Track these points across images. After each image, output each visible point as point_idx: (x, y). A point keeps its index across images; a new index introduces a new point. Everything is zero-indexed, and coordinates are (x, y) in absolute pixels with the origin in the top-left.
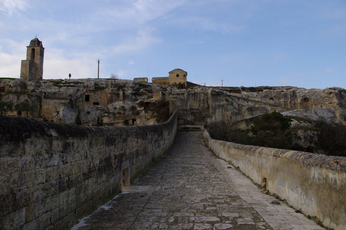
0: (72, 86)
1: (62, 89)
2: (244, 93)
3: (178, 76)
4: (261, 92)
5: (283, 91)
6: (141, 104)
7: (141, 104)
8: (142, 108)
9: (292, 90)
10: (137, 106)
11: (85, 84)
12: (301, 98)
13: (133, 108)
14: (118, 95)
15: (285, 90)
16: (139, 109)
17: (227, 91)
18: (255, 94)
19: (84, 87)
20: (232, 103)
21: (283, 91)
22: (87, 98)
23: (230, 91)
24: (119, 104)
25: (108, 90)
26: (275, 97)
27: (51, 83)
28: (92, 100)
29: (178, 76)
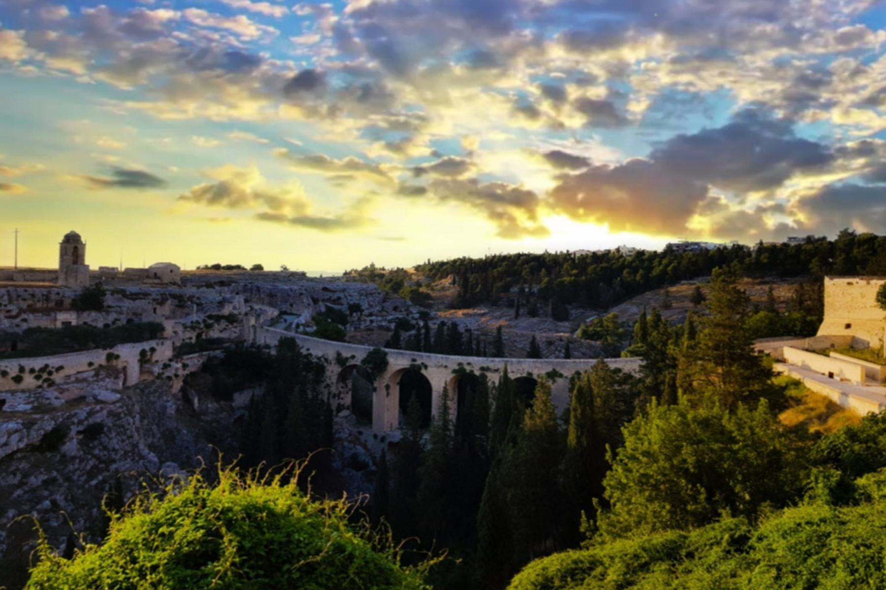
0: (141, 299)
13: (204, 321)
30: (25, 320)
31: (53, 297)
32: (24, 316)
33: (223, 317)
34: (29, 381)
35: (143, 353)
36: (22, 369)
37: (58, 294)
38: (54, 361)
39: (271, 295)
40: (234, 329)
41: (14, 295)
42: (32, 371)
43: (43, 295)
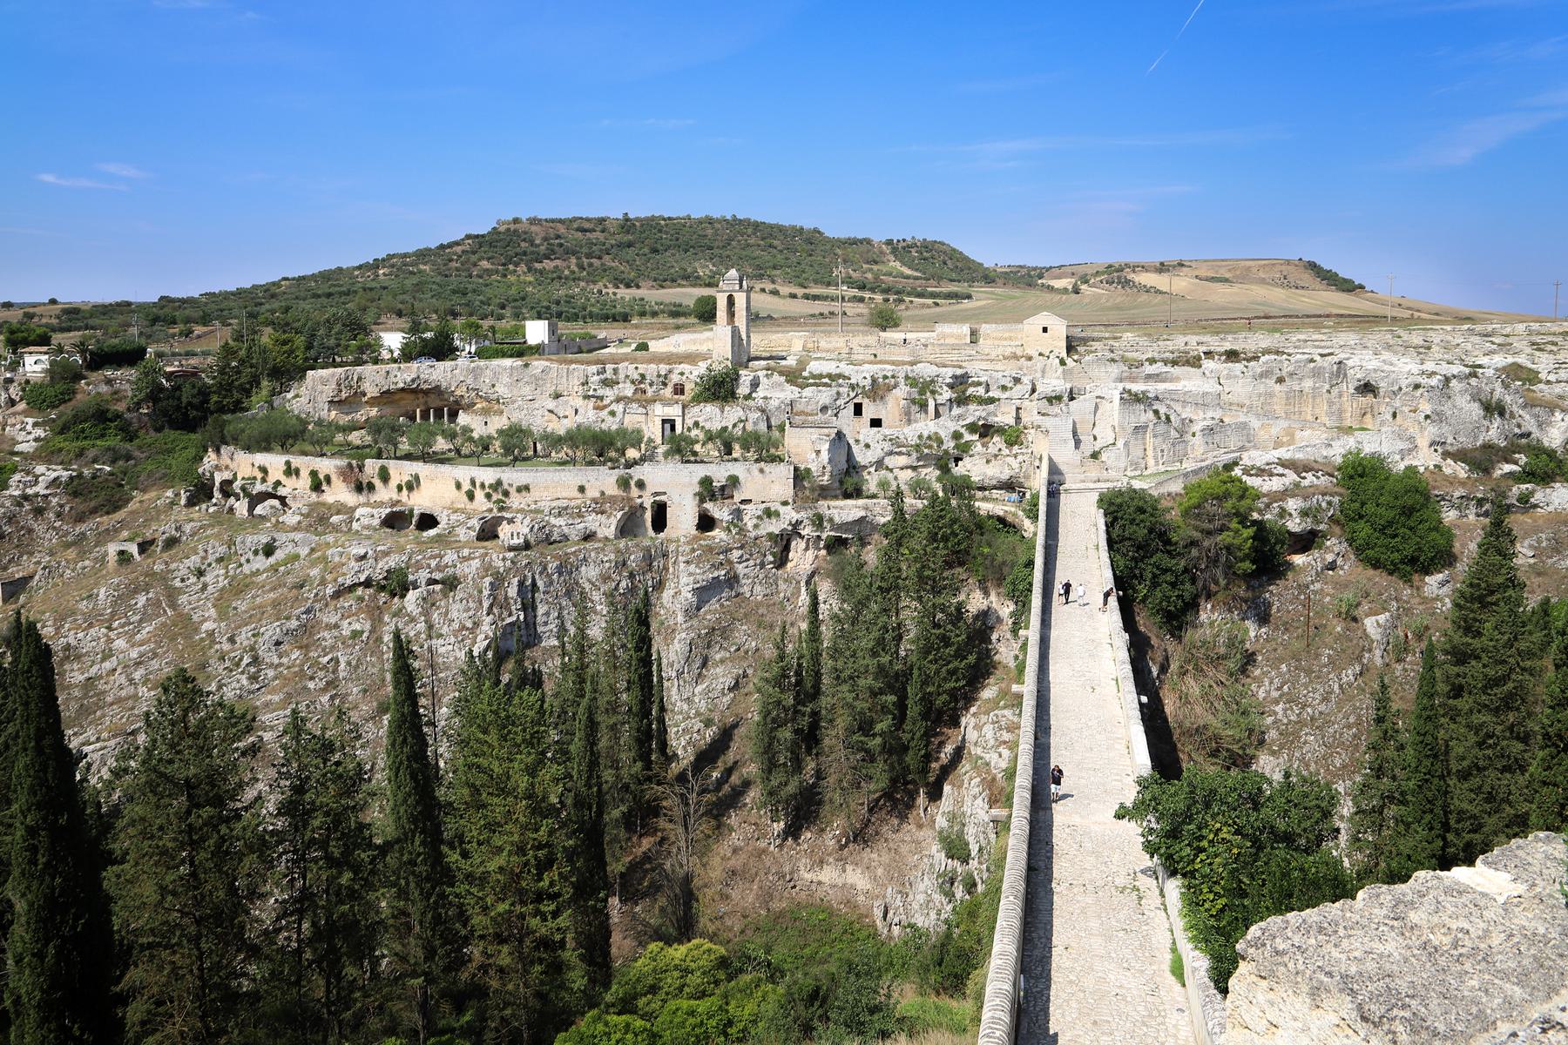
0: (825, 385)
1: (808, 392)
2: (1208, 364)
3: (1045, 330)
4: (1252, 363)
5: (1312, 361)
6: (972, 428)
7: (972, 428)
8: (976, 437)
9: (1336, 359)
10: (963, 430)
11: (853, 381)
12: (1357, 384)
13: (957, 436)
14: (923, 406)
15: (1318, 358)
16: (968, 437)
17: (1166, 362)
18: (1238, 367)
19: (852, 387)
20: (1168, 418)
21: (1312, 361)
22: (858, 410)
23: (1174, 363)
24: (926, 426)
25: (902, 391)
26: (1291, 375)
27: (783, 379)
28: (870, 411)
29: (1045, 330)
30: (613, 414)
31: (675, 378)
32: (614, 407)
33: (1000, 430)
34: (479, 495)
35: (706, 482)
36: (473, 483)
37: (682, 374)
38: (513, 476)
39: (1367, 388)
40: (1010, 460)
41: (622, 376)
42: (483, 486)
43: (659, 376)
